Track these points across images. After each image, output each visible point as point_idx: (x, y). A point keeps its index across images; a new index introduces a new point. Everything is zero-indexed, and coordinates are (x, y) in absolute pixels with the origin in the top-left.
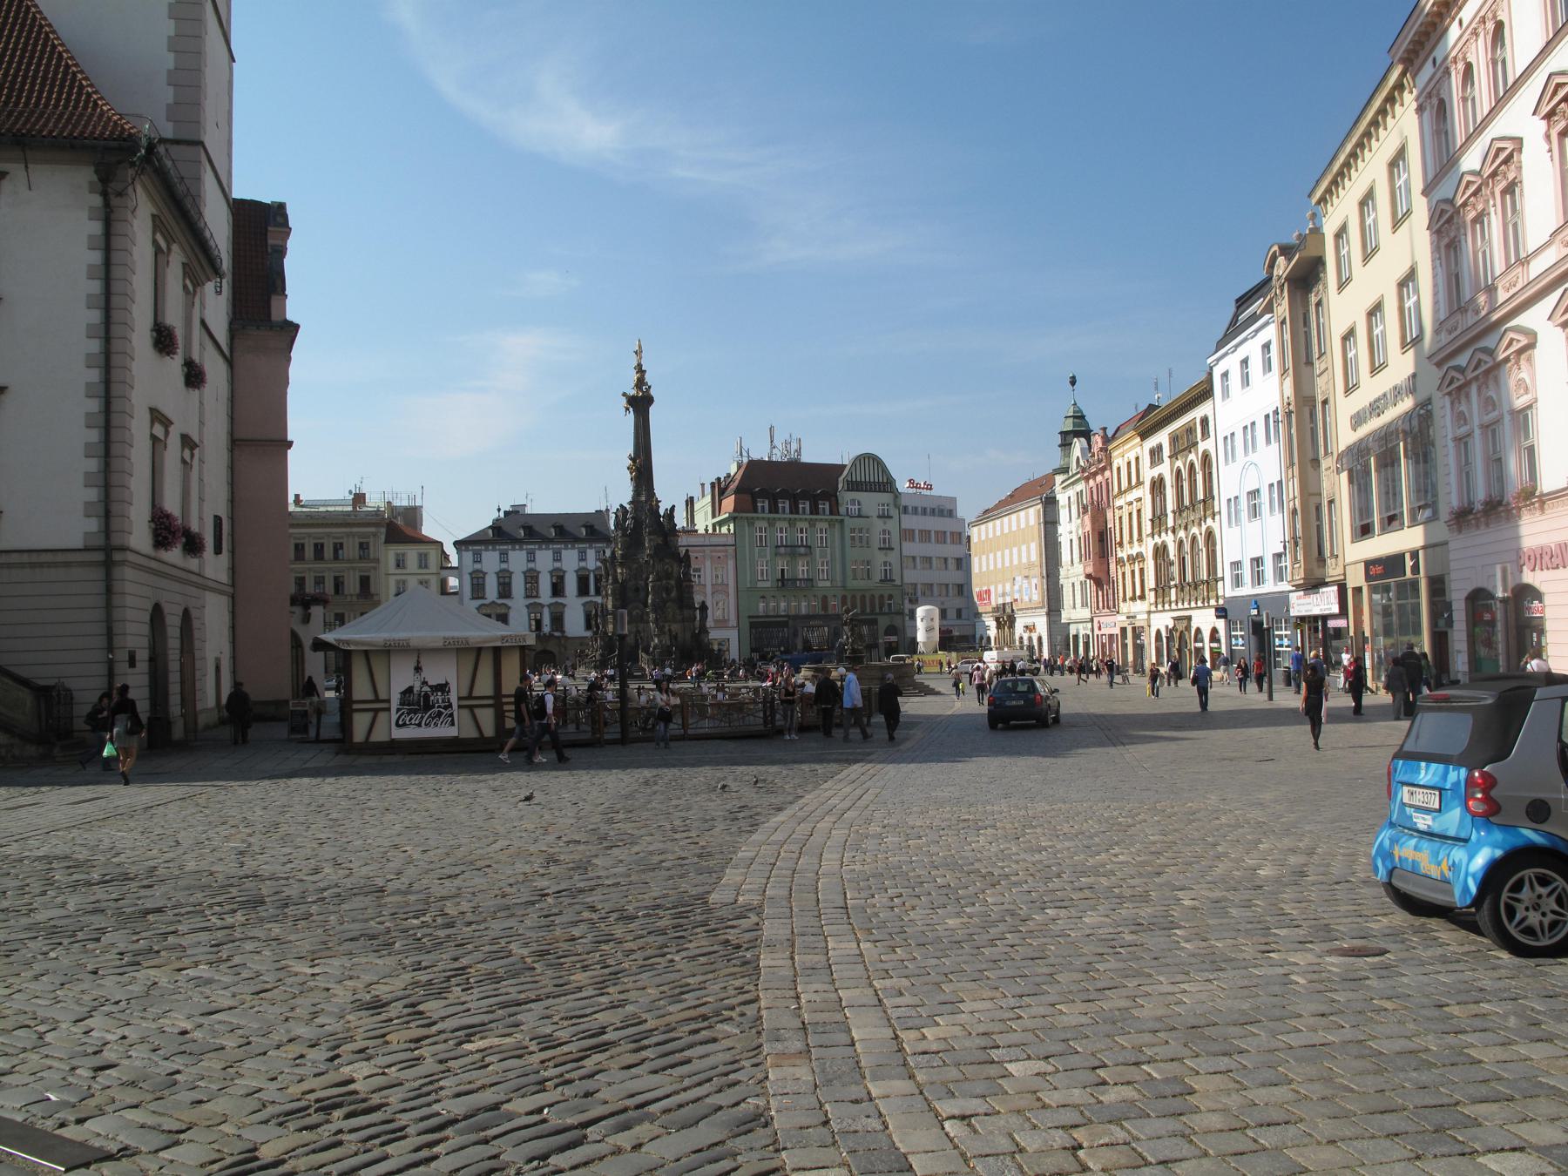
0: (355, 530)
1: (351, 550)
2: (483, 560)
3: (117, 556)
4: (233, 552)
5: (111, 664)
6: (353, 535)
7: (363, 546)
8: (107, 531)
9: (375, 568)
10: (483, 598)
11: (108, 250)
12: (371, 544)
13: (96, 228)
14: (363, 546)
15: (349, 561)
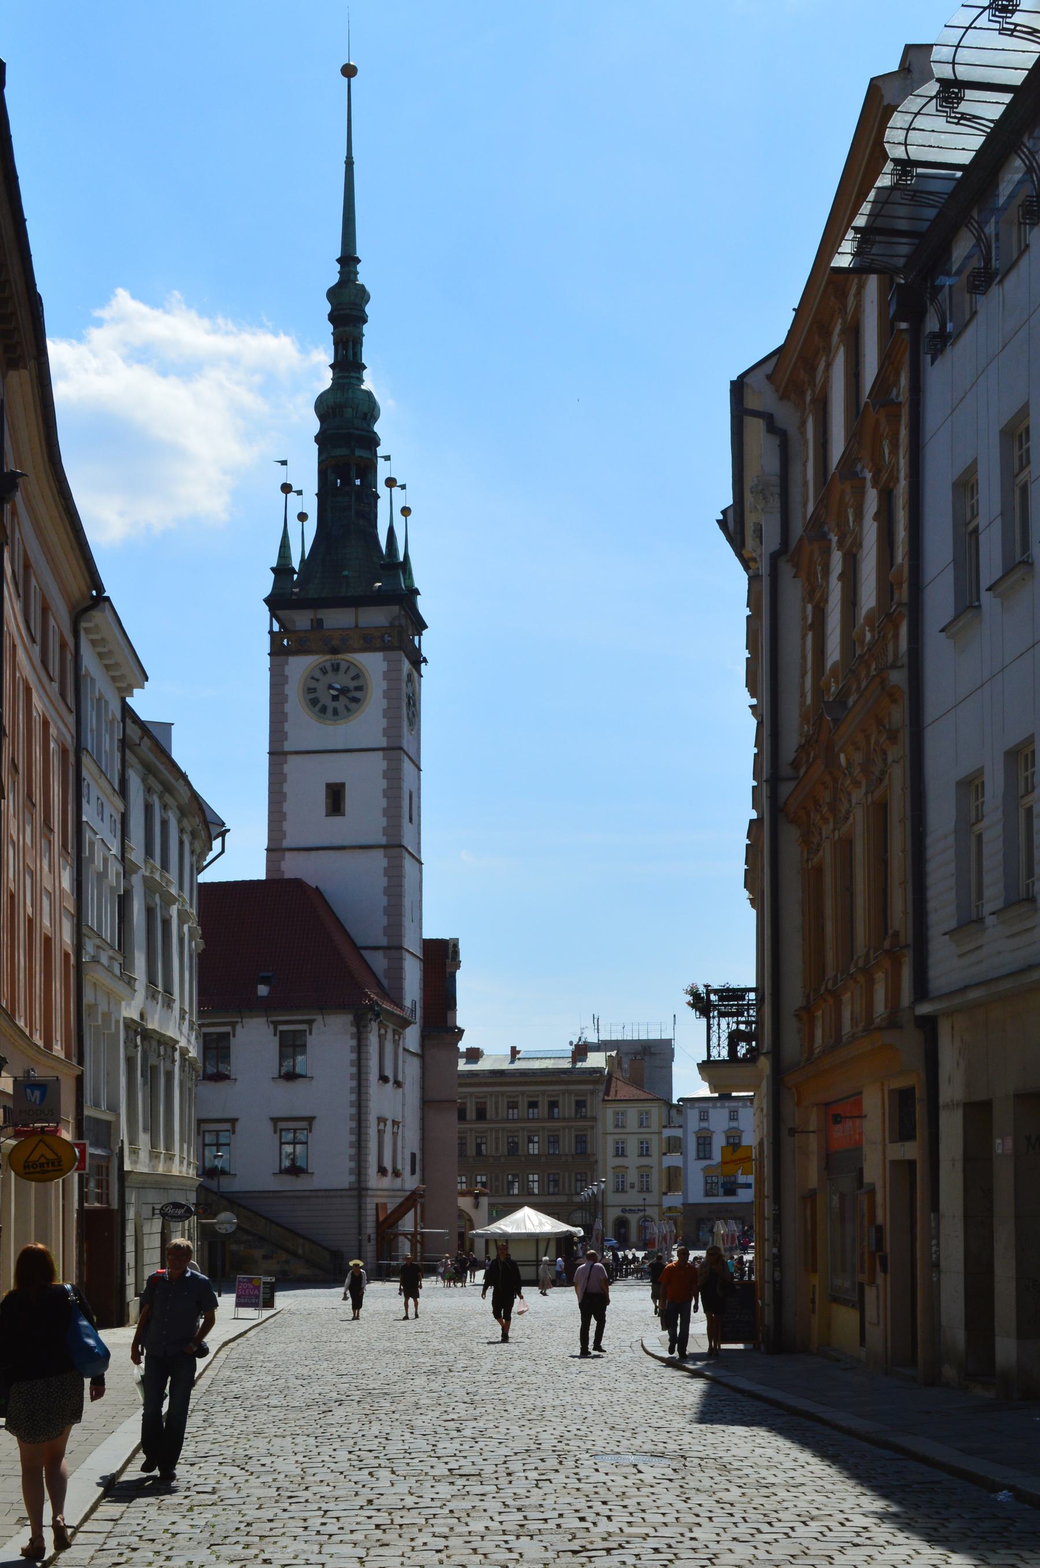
0: (571, 1087)
1: (566, 1108)
2: (710, 1118)
3: (363, 1193)
4: (423, 1170)
5: (360, 1241)
6: (570, 1092)
7: (580, 1104)
8: (359, 1181)
9: (592, 1128)
10: (710, 1158)
11: (359, 1053)
12: (588, 1103)
13: (354, 1043)
14: (580, 1104)
15: (564, 1119)
